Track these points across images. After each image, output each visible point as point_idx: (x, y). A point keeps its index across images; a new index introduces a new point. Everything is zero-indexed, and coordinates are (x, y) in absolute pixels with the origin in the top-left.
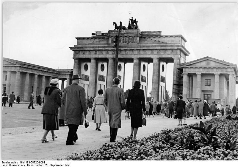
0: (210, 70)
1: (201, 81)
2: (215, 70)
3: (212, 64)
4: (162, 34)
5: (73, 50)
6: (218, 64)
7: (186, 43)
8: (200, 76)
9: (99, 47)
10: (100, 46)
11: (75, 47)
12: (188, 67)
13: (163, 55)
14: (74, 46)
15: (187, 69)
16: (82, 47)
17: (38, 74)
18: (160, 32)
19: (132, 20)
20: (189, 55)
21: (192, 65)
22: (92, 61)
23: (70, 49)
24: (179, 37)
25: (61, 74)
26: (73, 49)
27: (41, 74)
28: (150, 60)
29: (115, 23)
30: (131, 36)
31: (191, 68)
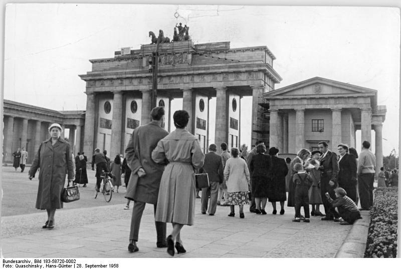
0: (321, 101)
1: (305, 124)
2: (332, 101)
3: (326, 91)
4: (232, 47)
5: (85, 80)
6: (339, 91)
7: (274, 61)
8: (303, 114)
9: (126, 73)
10: (128, 71)
11: (89, 75)
12: (278, 97)
13: (234, 82)
14: (86, 74)
15: (277, 103)
16: (99, 75)
17: (29, 118)
18: (227, 43)
19: (180, 28)
20: (281, 82)
21: (287, 94)
22: (116, 96)
23: (80, 78)
24: (262, 50)
25: (67, 118)
26: (85, 78)
27: (33, 118)
28: (210, 92)
29: (151, 34)
30: (178, 53)
31: (284, 99)
